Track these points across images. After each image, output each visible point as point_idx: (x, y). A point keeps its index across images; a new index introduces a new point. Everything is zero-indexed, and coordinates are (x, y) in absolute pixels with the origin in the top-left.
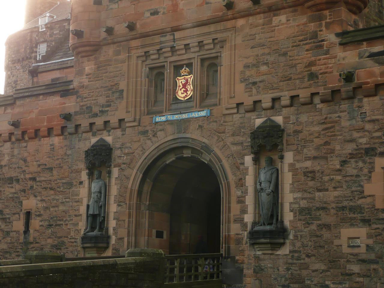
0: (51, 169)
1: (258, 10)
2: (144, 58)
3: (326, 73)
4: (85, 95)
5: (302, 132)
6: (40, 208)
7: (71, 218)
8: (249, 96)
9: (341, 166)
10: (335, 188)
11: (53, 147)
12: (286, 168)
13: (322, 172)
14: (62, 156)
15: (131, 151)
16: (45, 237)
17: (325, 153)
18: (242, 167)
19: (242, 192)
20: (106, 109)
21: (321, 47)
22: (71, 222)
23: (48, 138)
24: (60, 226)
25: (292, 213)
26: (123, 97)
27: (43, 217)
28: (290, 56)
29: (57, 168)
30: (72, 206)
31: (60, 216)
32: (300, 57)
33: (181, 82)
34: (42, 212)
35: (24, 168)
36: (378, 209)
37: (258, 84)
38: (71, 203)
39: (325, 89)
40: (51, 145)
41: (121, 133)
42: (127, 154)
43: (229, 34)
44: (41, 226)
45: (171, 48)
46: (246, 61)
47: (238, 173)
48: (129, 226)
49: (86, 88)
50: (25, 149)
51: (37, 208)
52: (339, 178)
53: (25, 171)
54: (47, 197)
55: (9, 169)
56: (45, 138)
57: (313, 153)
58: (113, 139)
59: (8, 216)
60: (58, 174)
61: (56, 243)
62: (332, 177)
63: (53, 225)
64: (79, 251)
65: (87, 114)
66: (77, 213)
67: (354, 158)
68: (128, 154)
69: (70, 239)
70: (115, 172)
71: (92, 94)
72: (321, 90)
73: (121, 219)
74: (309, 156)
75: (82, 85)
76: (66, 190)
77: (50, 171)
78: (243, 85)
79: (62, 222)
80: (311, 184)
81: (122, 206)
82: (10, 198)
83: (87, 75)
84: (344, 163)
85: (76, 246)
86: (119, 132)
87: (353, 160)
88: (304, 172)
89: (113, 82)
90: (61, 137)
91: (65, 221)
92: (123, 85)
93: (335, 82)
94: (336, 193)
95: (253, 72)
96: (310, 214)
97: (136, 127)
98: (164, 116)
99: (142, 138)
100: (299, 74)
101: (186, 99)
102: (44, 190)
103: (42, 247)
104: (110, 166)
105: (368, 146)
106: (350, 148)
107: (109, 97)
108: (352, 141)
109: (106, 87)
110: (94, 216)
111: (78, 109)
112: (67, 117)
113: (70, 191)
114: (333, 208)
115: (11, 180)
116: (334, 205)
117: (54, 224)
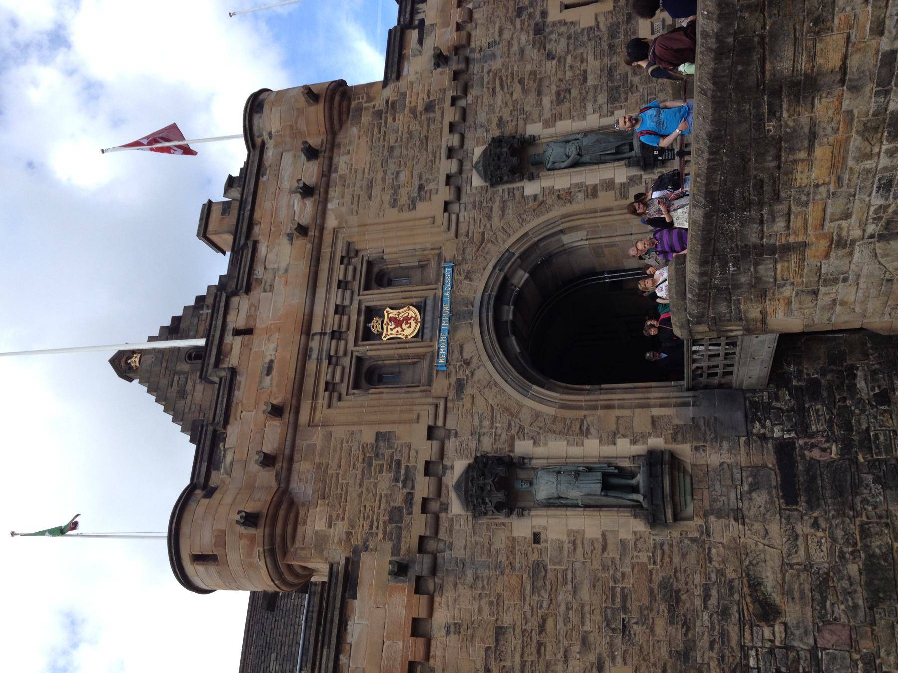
0: (500, 631)
2: (335, 395)
3: (429, 91)
4: (366, 527)
6: (582, 665)
7: (610, 562)
9: (553, 58)
10: (582, 62)
11: (453, 628)
12: (551, 131)
13: (561, 80)
14: (475, 599)
16: (651, 643)
18: (540, 198)
19: (579, 191)
20: (403, 471)
21: (394, 103)
22: (618, 563)
23: (433, 642)
24: (626, 596)
27: (605, 655)
28: (396, 141)
29: (498, 613)
30: (584, 563)
31: (604, 597)
32: (400, 129)
33: (392, 329)
34: (592, 658)
36: (614, 7)
37: (423, 182)
39: (449, 90)
40: (448, 632)
41: (453, 439)
42: (493, 419)
43: (340, 236)
44: (624, 659)
45: (332, 338)
46: (386, 205)
47: (549, 202)
48: (630, 407)
49: (353, 527)
52: (569, 59)
54: (559, 641)
56: (432, 653)
57: (532, 98)
60: (512, 609)
61: (663, 607)
63: (623, 620)
64: (681, 534)
66: (598, 546)
67: (545, 44)
69: (654, 563)
70: (523, 447)
71: (367, 510)
72: (449, 94)
73: (613, 427)
74: (535, 102)
75: (344, 537)
76: (548, 583)
77: (504, 634)
78: (420, 205)
79: (618, 590)
80: (574, 92)
84: (550, 56)
85: (671, 546)
86: (451, 445)
87: (548, 47)
88: (558, 105)
89: (357, 459)
90: (437, 599)
92: (368, 436)
93: (443, 77)
94: (590, 58)
95: (403, 192)
96: (618, 87)
97: (448, 405)
98: (438, 348)
99: (469, 391)
102: (543, 648)
103: (674, 654)
104: (511, 458)
105: (531, 33)
106: (532, 53)
107: (383, 465)
108: (522, 51)
110: (607, 487)
111: (388, 546)
112: (400, 570)
114: (610, 60)
116: (606, 60)
117: (623, 616)
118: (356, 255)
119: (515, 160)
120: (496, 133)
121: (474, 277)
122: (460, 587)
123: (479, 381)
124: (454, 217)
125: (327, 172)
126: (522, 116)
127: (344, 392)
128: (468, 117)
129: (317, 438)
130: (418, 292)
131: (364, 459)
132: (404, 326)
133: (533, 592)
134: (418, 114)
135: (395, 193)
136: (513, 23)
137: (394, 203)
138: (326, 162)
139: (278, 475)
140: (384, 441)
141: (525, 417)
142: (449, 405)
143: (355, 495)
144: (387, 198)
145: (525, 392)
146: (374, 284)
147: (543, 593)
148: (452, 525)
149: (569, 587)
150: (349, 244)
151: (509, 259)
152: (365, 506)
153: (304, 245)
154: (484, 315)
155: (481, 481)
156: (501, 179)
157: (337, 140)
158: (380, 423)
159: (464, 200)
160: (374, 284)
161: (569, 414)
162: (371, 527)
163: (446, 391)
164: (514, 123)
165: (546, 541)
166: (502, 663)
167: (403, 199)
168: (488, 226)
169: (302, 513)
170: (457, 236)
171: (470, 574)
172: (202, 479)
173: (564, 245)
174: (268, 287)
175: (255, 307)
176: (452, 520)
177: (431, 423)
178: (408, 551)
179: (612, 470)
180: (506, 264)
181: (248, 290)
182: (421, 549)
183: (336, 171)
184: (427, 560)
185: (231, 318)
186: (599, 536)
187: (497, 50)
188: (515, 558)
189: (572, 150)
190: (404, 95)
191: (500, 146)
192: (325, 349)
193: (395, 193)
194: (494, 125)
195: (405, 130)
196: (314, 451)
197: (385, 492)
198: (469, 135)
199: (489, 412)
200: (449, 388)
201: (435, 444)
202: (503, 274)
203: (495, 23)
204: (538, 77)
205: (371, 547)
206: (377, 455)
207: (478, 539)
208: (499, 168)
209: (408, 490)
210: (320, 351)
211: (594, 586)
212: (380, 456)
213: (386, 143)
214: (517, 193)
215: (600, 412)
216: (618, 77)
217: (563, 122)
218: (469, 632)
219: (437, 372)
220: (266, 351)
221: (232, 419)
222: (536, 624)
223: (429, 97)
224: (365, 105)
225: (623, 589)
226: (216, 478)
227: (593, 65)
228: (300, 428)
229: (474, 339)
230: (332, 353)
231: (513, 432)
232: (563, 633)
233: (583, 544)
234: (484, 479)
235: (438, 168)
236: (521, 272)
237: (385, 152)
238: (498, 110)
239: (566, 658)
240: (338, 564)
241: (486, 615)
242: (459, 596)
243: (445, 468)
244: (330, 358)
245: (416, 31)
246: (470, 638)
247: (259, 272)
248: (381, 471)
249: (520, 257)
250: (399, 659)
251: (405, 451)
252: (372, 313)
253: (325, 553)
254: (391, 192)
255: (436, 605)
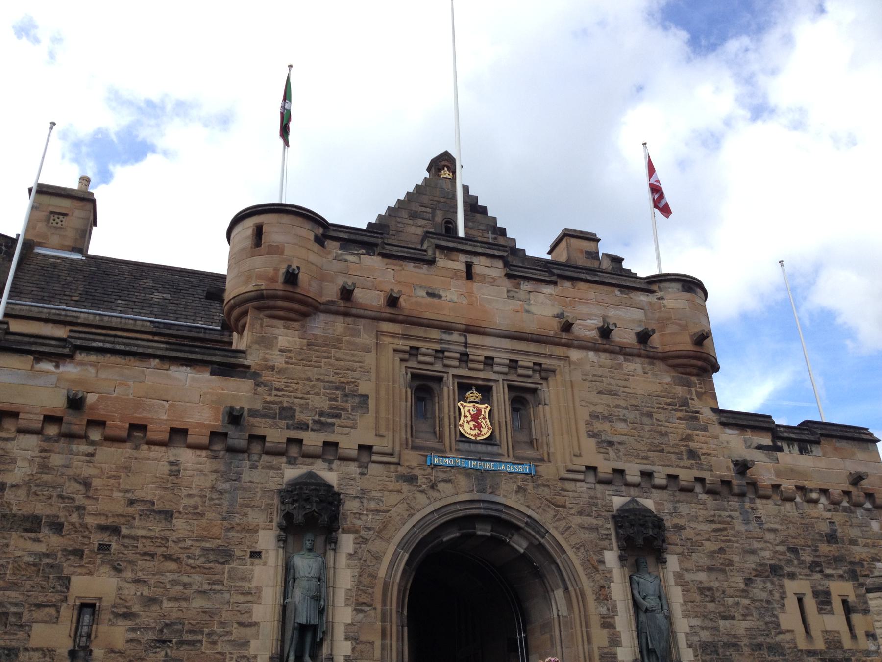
0: (168, 515)
1: (607, 346)
2: (406, 356)
3: (709, 454)
5: (685, 529)
6: (129, 597)
7: (228, 629)
8: (605, 459)
9: (746, 585)
10: (743, 615)
11: (175, 468)
12: (672, 581)
13: (724, 592)
15: (382, 507)
17: (722, 564)
18: (601, 568)
19: (608, 609)
20: (329, 420)
21: (696, 419)
22: (226, 638)
23: (163, 448)
25: (691, 650)
26: (368, 408)
27: (138, 621)
29: (186, 514)
30: (229, 602)
31: (194, 622)
32: (670, 425)
33: (469, 411)
34: (136, 608)
35: (80, 500)
37: (616, 445)
38: (227, 596)
40: (171, 464)
41: (358, 470)
44: (131, 641)
45: (461, 354)
46: (593, 408)
47: (598, 577)
49: (279, 372)
50: (88, 458)
51: (120, 599)
52: (746, 602)
53: (84, 509)
54: (154, 575)
55: (28, 495)
56: (153, 447)
57: (705, 561)
58: (341, 479)
59: (13, 609)
60: (188, 528)
62: (736, 599)
63: (170, 641)
65: (280, 419)
66: (244, 618)
68: (378, 511)
70: (347, 542)
71: (294, 386)
73: (363, 638)
74: (701, 564)
76: (212, 565)
77: (165, 519)
78: (592, 442)
79: (200, 637)
80: (711, 606)
81: (365, 612)
82: (28, 564)
83: (281, 351)
84: (748, 581)
86: (353, 469)
87: (758, 579)
88: (699, 588)
90: (204, 453)
91: (209, 635)
92: (365, 387)
95: (606, 426)
98: (449, 457)
99: (406, 487)
100: (673, 447)
101: (478, 439)
102: (149, 558)
104: (336, 530)
105: (772, 562)
106: (751, 562)
107: (337, 401)
108: (753, 552)
109: (328, 382)
110: (303, 629)
111: (258, 406)
112: (235, 418)
113: (224, 568)
115: (32, 524)
116: (746, 641)
117: (174, 641)
118: (542, 378)
119: (640, 541)
120: (668, 523)
121: (520, 496)
122: (214, 476)
123: (415, 498)
124: (581, 476)
125: (623, 351)
126: (686, 551)
127: (409, 364)
128: (684, 493)
129: (366, 338)
130: (505, 438)
131: (343, 383)
132: (472, 423)
133: (203, 549)
134: (685, 443)
135: (605, 418)
136: (782, 543)
137: (594, 416)
138: (635, 351)
139: (332, 302)
140: (359, 403)
141: (376, 546)
142: (392, 467)
143: (309, 374)
144: (600, 409)
145: (402, 545)
146: (513, 394)
147: (203, 559)
148: (274, 469)
149: (206, 587)
150: (554, 371)
151: (538, 532)
152: (298, 384)
153: (552, 328)
154: (481, 505)
155: (315, 499)
156: (621, 527)
157: (657, 362)
158: (377, 399)
159: (598, 486)
160: (513, 394)
161: (378, 592)
162: (278, 390)
163: (406, 464)
164: (678, 542)
165: (252, 564)
166: (137, 517)
167: (598, 426)
168: (572, 512)
169: (296, 324)
170: (561, 479)
171: (226, 486)
172: (332, 234)
173: (553, 591)
174: (511, 294)
175: (493, 282)
176: (280, 469)
177: (375, 449)
178: (253, 425)
179: (320, 635)
180: (533, 529)
181: (509, 276)
182: (253, 438)
183: (626, 360)
184: (243, 443)
185: (483, 260)
186: (254, 619)
187: (753, 526)
188: (238, 532)
189: (651, 602)
190: (705, 429)
191: (654, 526)
192: (452, 347)
193: (605, 418)
194: (675, 521)
195: (670, 430)
196: (352, 336)
197: (310, 403)
198: (665, 495)
199: (383, 508)
200: (409, 468)
201: (354, 453)
202: (523, 525)
203: (781, 524)
204: (727, 568)
205: (259, 389)
206: (346, 395)
207: (259, 495)
208: (632, 525)
209: (310, 425)
210: (449, 342)
211: (205, 612)
212: (345, 399)
213: (655, 410)
214: (606, 543)
215: (379, 624)
216: (728, 653)
217: (680, 593)
218: (170, 485)
219: (426, 456)
220: (450, 292)
221: (387, 260)
222: (172, 552)
223: (703, 454)
224: (693, 390)
225: (201, 642)
226: (333, 247)
227: (741, 627)
228: (375, 323)
229: (457, 493)
230: (446, 354)
231: (363, 532)
232: (162, 579)
233: (248, 602)
234: (316, 502)
235: (630, 462)
236: (525, 544)
237: (646, 409)
238: (691, 525)
239: (137, 581)
240: (245, 358)
241: (185, 501)
242: (205, 475)
243: (330, 462)
244: (442, 351)
245: (771, 444)
246: (164, 485)
247: (526, 286)
248: (330, 399)
249: (540, 544)
250: (150, 416)
251: (349, 423)
252: (486, 392)
253: (257, 346)
254: (606, 413)
255: (199, 452)
